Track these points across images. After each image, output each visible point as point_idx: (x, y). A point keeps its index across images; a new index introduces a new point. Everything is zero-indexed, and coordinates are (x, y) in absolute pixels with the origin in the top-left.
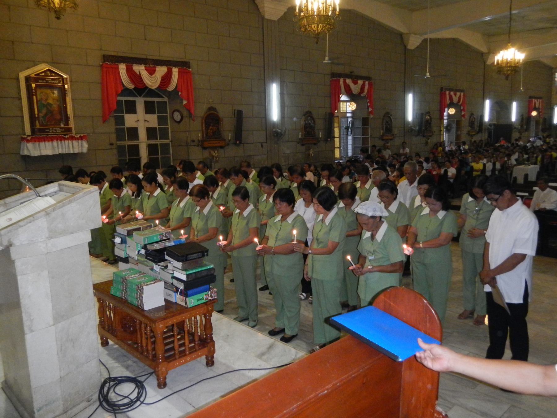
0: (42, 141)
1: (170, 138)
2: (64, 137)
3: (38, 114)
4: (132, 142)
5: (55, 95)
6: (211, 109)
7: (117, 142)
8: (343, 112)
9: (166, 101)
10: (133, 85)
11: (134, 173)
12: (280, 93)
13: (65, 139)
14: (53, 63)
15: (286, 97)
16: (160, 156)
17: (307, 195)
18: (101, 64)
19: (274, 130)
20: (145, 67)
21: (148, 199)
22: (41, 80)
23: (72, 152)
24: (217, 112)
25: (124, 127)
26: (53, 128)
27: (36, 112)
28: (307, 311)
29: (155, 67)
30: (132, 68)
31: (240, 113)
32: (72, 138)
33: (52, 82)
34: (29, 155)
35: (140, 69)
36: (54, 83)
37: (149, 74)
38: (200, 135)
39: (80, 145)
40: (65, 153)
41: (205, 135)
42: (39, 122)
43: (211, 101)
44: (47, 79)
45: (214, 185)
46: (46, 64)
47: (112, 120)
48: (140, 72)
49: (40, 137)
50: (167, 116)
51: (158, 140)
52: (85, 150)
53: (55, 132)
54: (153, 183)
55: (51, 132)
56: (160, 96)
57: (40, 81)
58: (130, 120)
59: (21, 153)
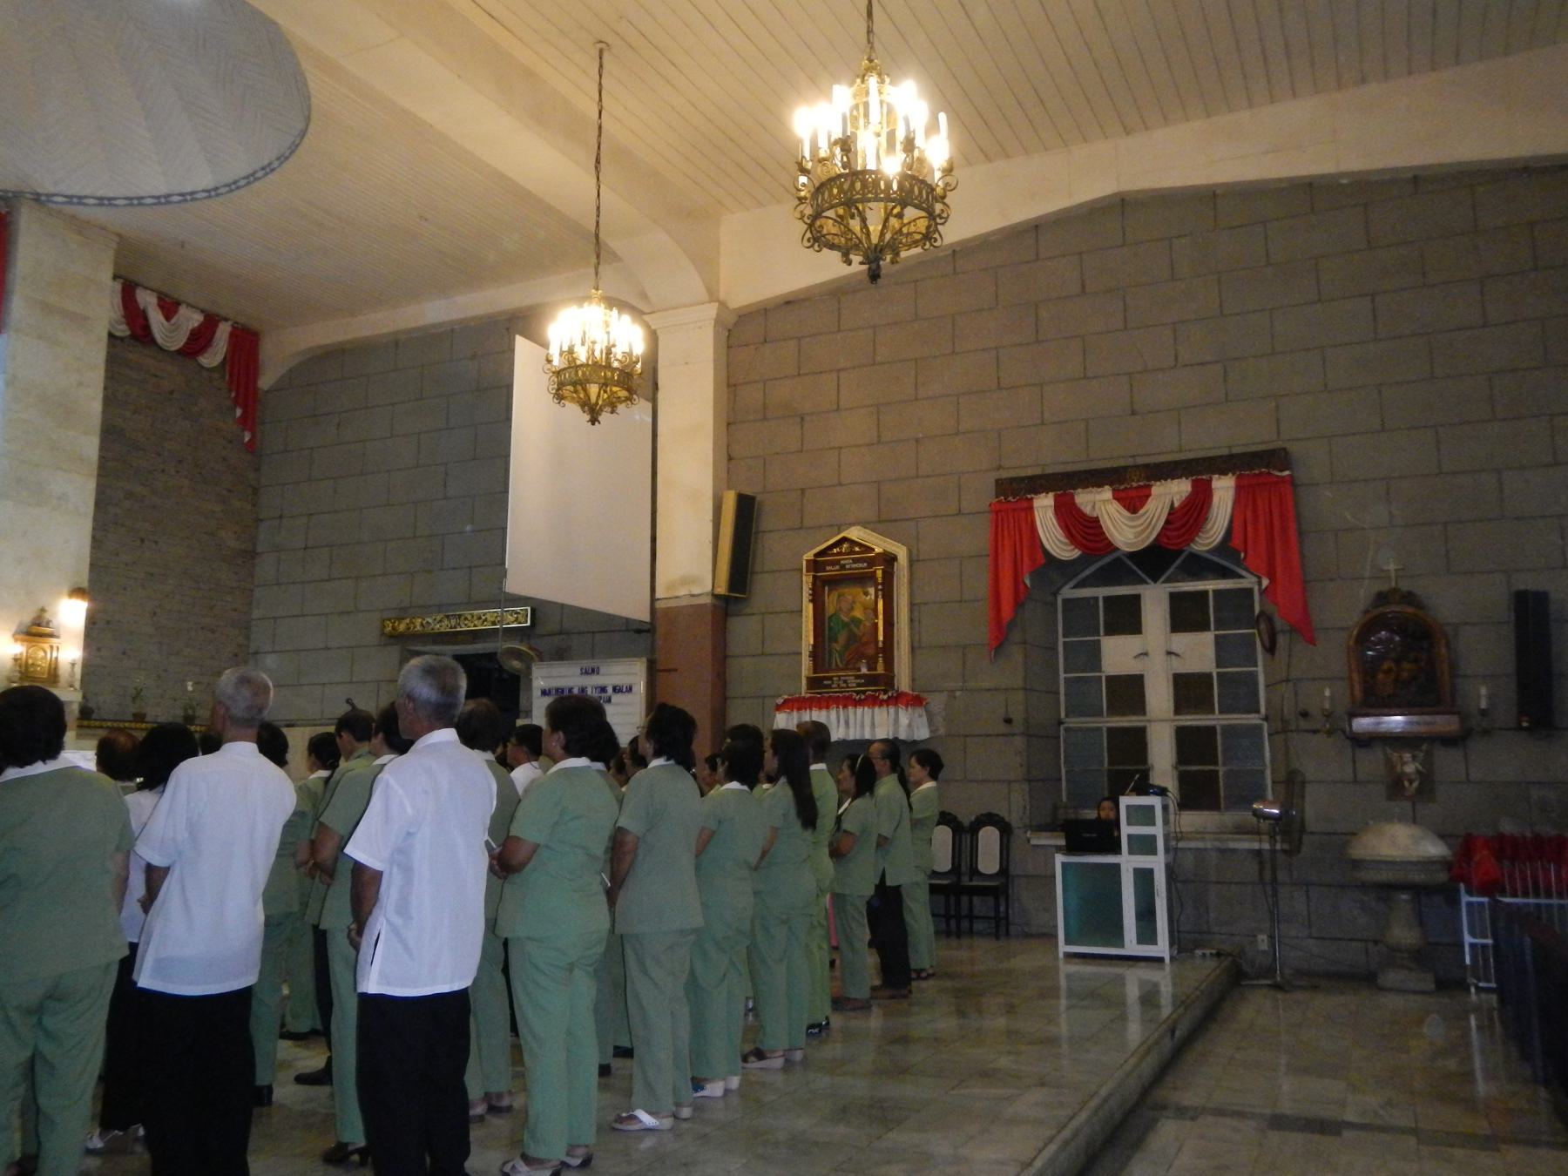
1: (1263, 710)
4: (1124, 719)
5: (868, 598)
9: (1249, 586)
10: (1077, 550)
16: (1221, 770)
26: (839, 677)
29: (1149, 487)
30: (1073, 499)
33: (854, 566)
35: (1099, 502)
36: (856, 569)
41: (1358, 693)
44: (842, 562)
46: (859, 527)
53: (844, 685)
55: (834, 686)
56: (1225, 573)
57: (828, 568)
58: (1118, 654)
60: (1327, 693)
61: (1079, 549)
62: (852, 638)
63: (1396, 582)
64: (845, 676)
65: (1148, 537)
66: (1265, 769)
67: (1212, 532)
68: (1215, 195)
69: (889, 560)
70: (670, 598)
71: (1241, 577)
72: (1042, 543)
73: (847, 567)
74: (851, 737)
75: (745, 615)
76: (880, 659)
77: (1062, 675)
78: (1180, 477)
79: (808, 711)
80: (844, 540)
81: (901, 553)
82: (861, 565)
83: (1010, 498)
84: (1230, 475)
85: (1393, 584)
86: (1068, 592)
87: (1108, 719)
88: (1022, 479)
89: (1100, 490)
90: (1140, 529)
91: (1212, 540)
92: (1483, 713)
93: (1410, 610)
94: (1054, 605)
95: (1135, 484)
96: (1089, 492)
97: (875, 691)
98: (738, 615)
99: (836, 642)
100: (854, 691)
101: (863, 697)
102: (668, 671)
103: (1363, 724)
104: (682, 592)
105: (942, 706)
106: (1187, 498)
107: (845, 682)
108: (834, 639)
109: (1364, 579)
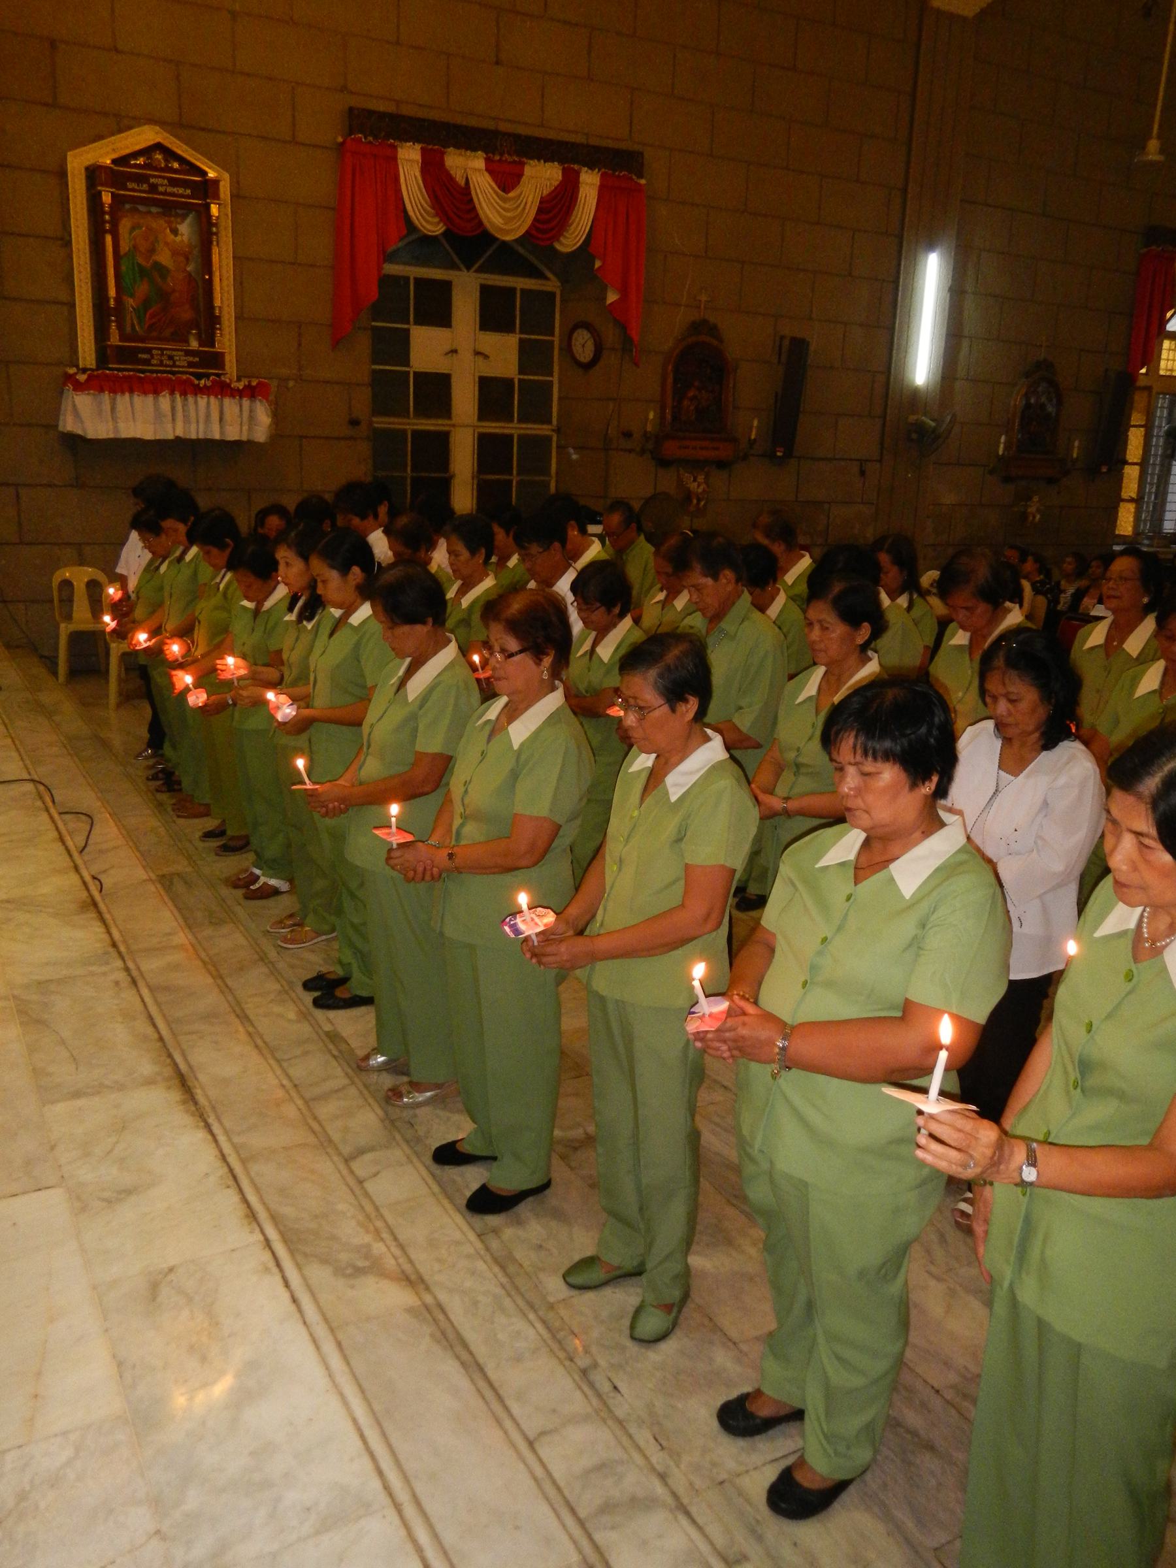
0: (123, 392)
2: (196, 382)
3: (118, 299)
5: (178, 239)
6: (700, 327)
7: (374, 419)
8: (1168, 373)
9: (553, 289)
11: (356, 521)
13: (198, 391)
15: (969, 303)
17: (1024, 706)
18: (340, 139)
19: (912, 418)
20: (488, 160)
21: (331, 635)
22: (132, 181)
23: (217, 436)
24: (721, 341)
25: (407, 369)
27: (112, 292)
28: (938, 1279)
31: (797, 350)
32: (222, 389)
33: (170, 189)
34: (80, 432)
37: (499, 187)
38: (651, 415)
39: (246, 414)
40: (194, 436)
41: (669, 417)
42: (120, 327)
43: (704, 298)
44: (152, 180)
45: (615, 606)
47: (363, 345)
48: (467, 179)
49: (117, 377)
50: (553, 341)
51: (515, 424)
52: (261, 434)
53: (170, 363)
54: (356, 570)
55: (154, 362)
56: (535, 274)
57: (130, 185)
59: (61, 428)
61: (445, 224)
64: (170, 349)
66: (550, 480)
71: (546, 278)
72: (404, 205)
79: (127, 395)
82: (181, 191)
87: (415, 421)
107: (171, 358)
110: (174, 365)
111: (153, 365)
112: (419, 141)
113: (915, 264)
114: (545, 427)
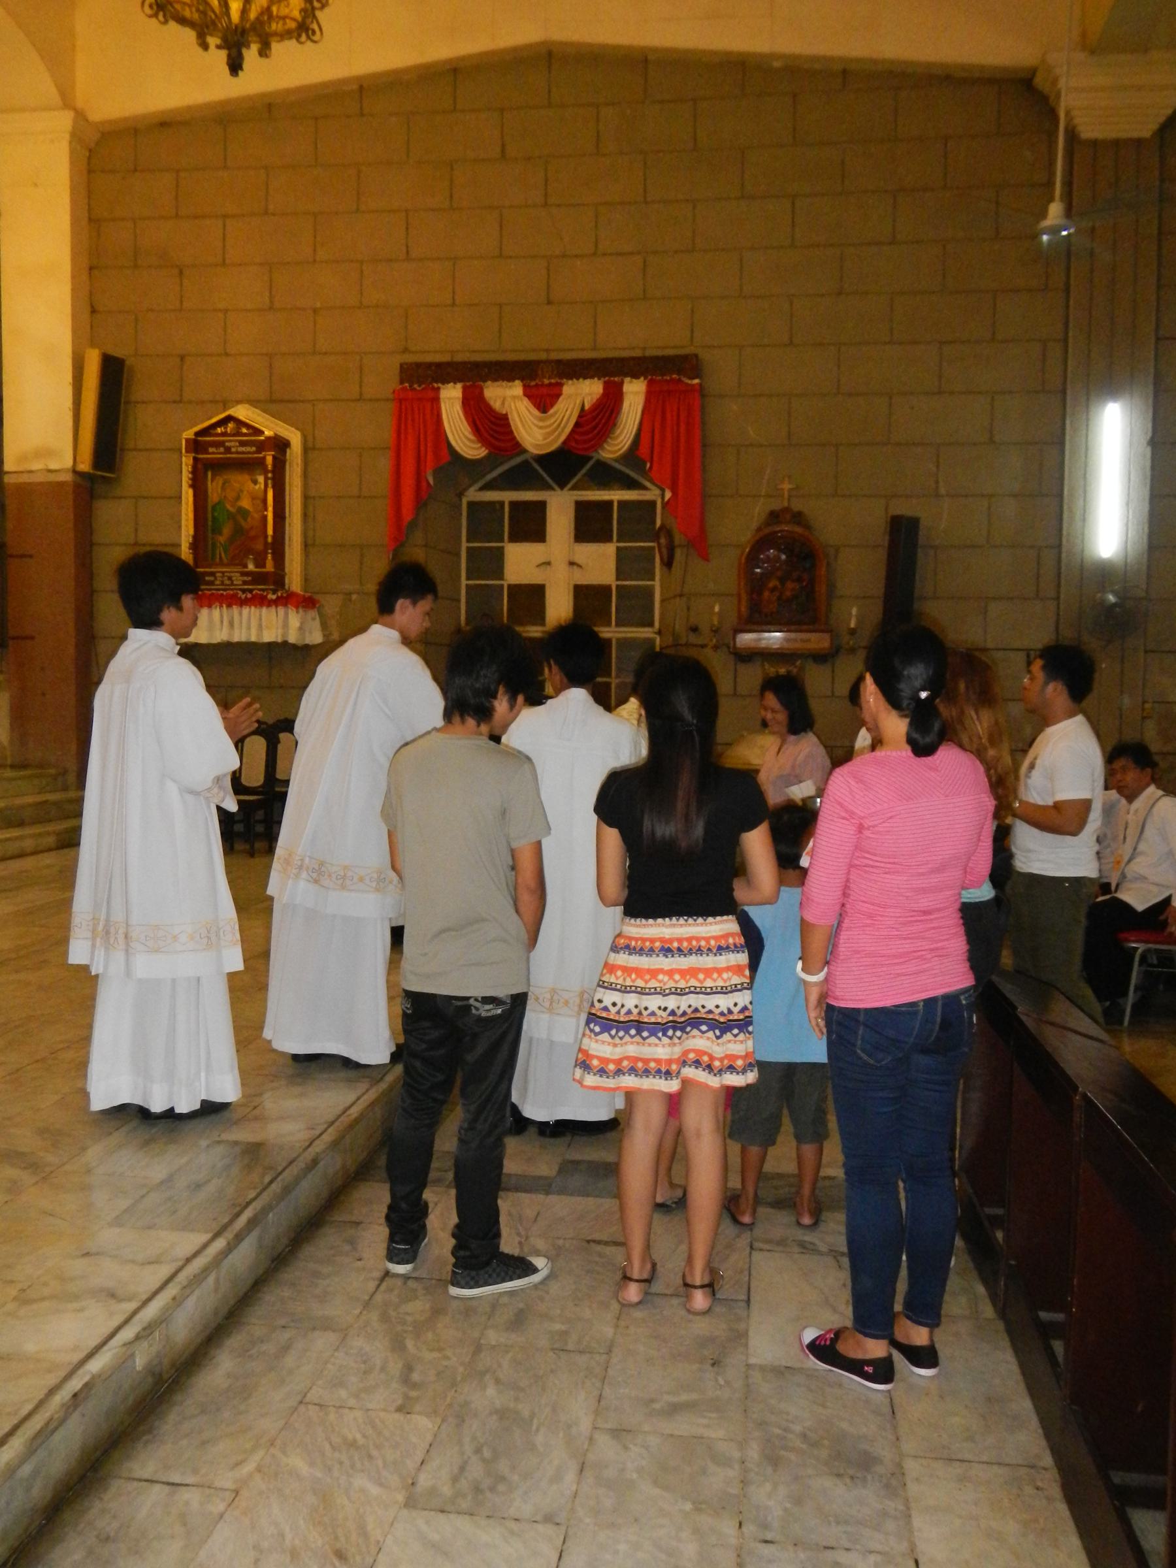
1: (657, 624)
5: (257, 487)
10: (484, 449)
12: (1153, 443)
14: (272, 401)
20: (525, 387)
24: (807, 527)
26: (223, 573)
29: (561, 385)
44: (227, 444)
46: (247, 405)
51: (613, 628)
53: (228, 582)
56: (632, 484)
57: (211, 450)
60: (717, 609)
61: (486, 448)
62: (238, 531)
63: (789, 500)
64: (230, 572)
65: (555, 440)
67: (621, 439)
68: (646, 61)
69: (281, 445)
70: (22, 472)
71: (645, 488)
73: (233, 450)
74: (236, 639)
75: (114, 498)
76: (270, 555)
77: (464, 582)
78: (592, 377)
80: (229, 418)
81: (295, 439)
82: (248, 449)
83: (416, 386)
84: (642, 378)
85: (786, 504)
86: (474, 494)
88: (429, 365)
89: (510, 384)
90: (548, 430)
91: (620, 446)
92: (853, 632)
93: (798, 530)
94: (459, 507)
95: (546, 381)
96: (498, 386)
97: (263, 590)
98: (105, 498)
99: (220, 533)
100: (240, 590)
101: (249, 596)
102: (23, 556)
103: (746, 639)
104: (37, 466)
105: (337, 609)
106: (597, 400)
108: (217, 531)
109: (760, 496)
110: (232, 584)
111: (217, 585)
112: (460, 381)
113: (1088, 420)
114: (646, 629)
